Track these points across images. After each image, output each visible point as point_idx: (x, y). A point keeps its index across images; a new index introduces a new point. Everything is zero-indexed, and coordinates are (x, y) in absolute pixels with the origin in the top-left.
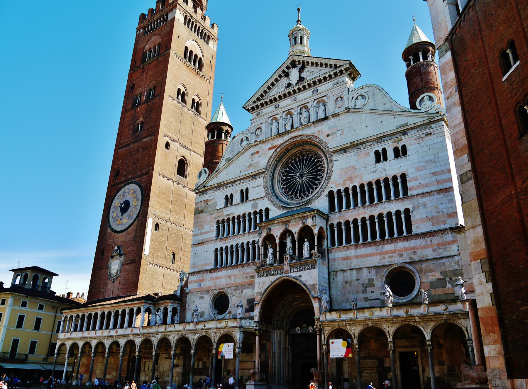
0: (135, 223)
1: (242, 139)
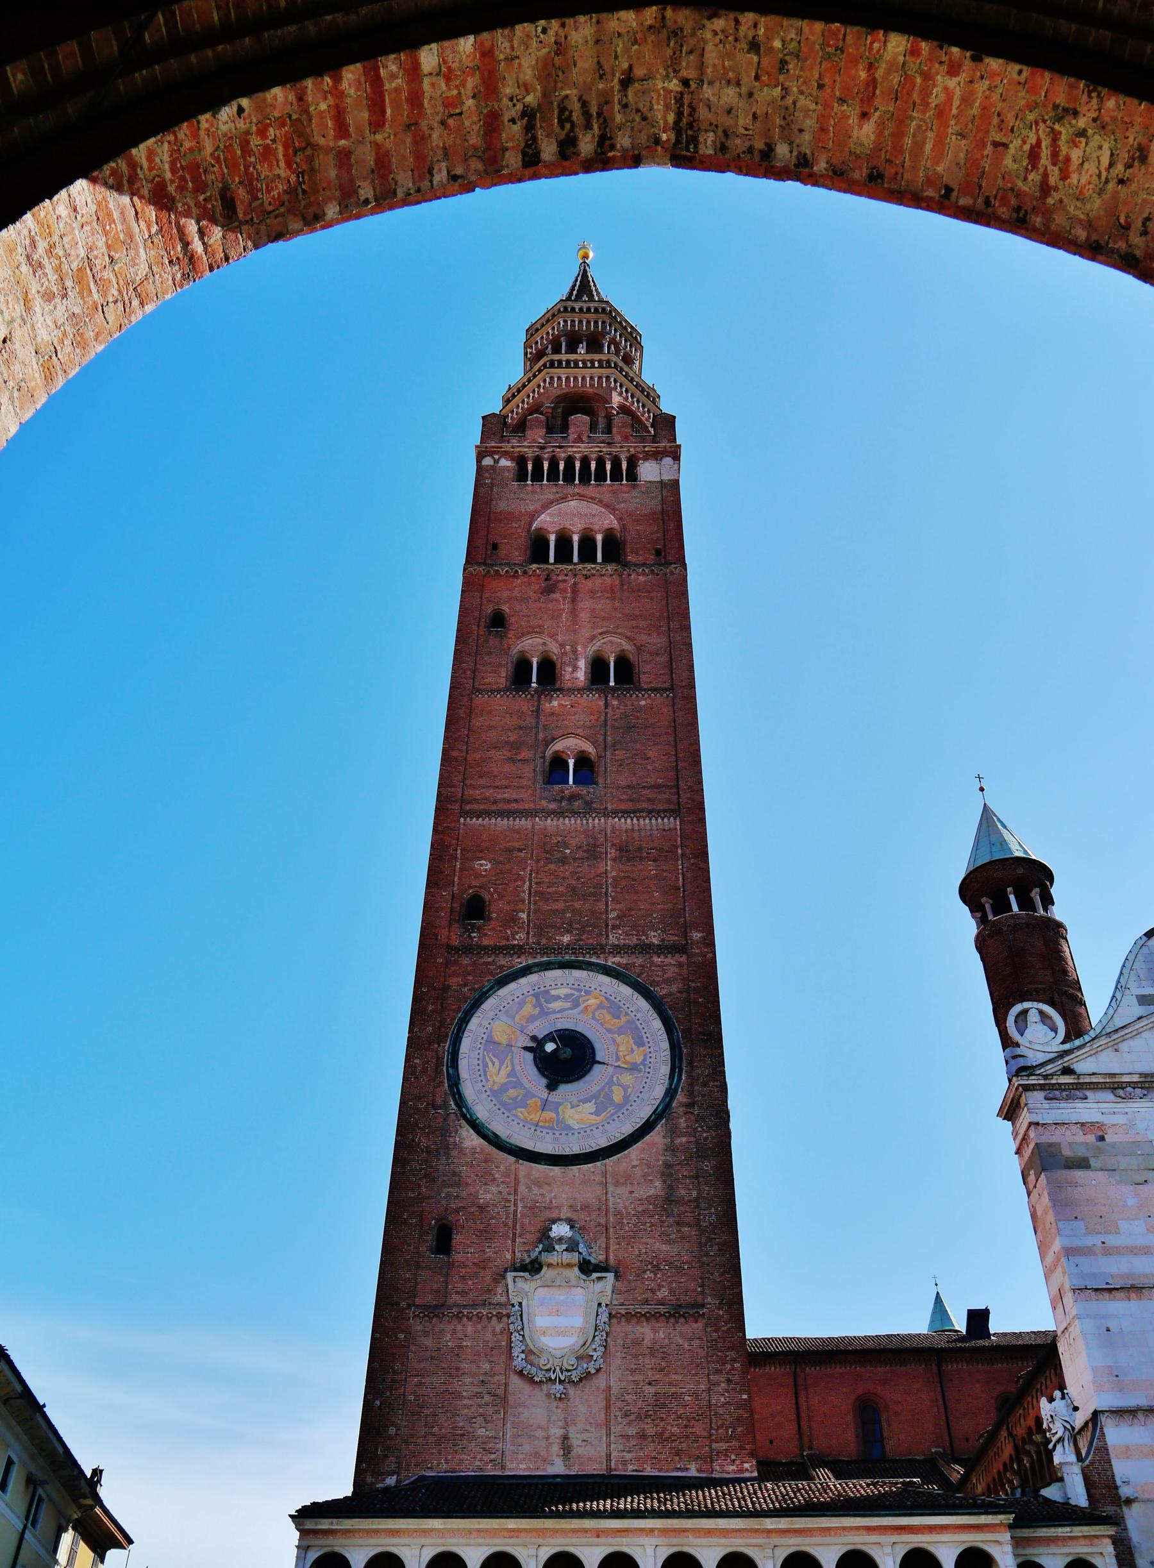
0: (656, 1137)
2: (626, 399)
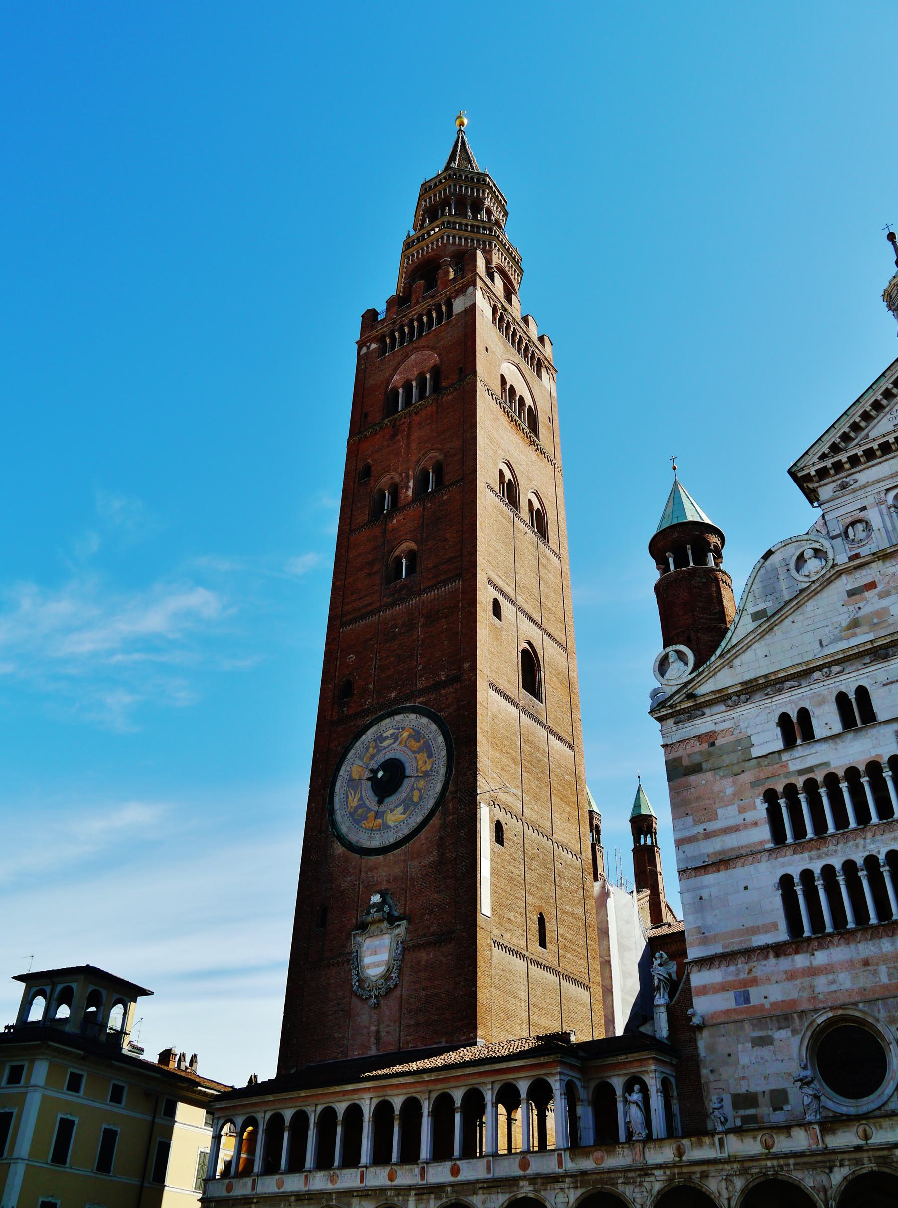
0: (435, 821)
1: (801, 555)
2: (460, 245)
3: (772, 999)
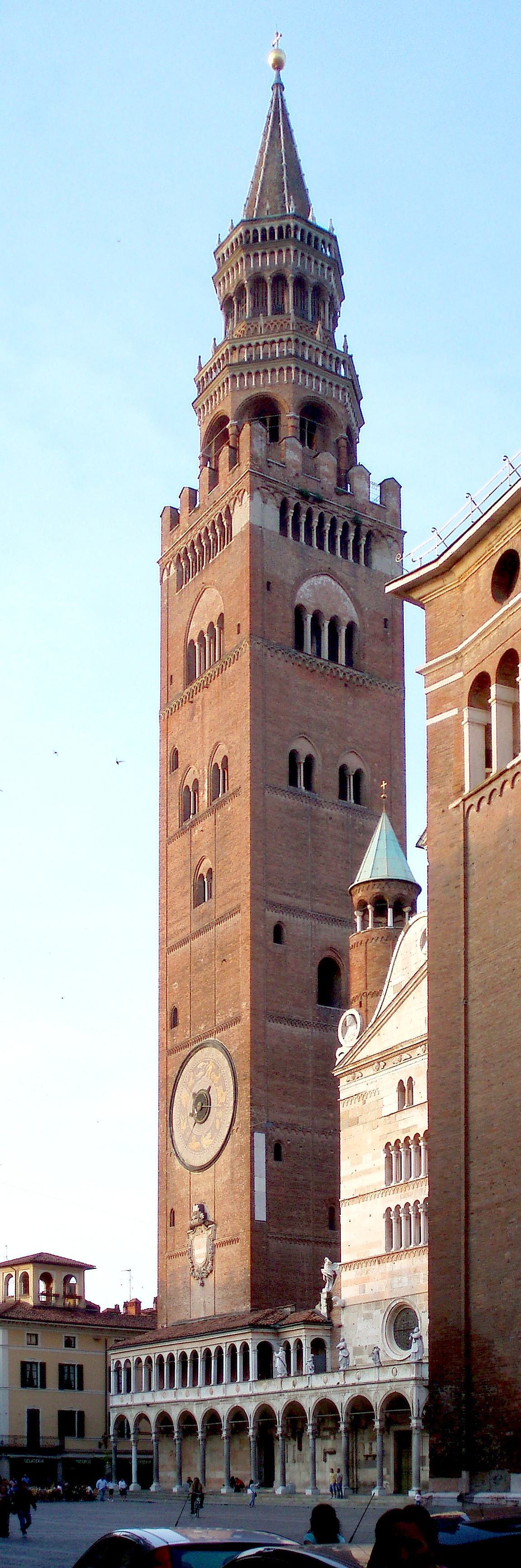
3: (374, 1291)
